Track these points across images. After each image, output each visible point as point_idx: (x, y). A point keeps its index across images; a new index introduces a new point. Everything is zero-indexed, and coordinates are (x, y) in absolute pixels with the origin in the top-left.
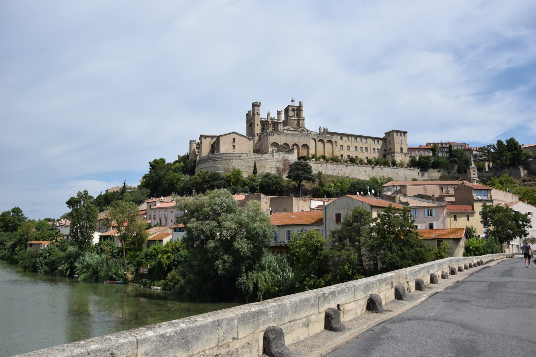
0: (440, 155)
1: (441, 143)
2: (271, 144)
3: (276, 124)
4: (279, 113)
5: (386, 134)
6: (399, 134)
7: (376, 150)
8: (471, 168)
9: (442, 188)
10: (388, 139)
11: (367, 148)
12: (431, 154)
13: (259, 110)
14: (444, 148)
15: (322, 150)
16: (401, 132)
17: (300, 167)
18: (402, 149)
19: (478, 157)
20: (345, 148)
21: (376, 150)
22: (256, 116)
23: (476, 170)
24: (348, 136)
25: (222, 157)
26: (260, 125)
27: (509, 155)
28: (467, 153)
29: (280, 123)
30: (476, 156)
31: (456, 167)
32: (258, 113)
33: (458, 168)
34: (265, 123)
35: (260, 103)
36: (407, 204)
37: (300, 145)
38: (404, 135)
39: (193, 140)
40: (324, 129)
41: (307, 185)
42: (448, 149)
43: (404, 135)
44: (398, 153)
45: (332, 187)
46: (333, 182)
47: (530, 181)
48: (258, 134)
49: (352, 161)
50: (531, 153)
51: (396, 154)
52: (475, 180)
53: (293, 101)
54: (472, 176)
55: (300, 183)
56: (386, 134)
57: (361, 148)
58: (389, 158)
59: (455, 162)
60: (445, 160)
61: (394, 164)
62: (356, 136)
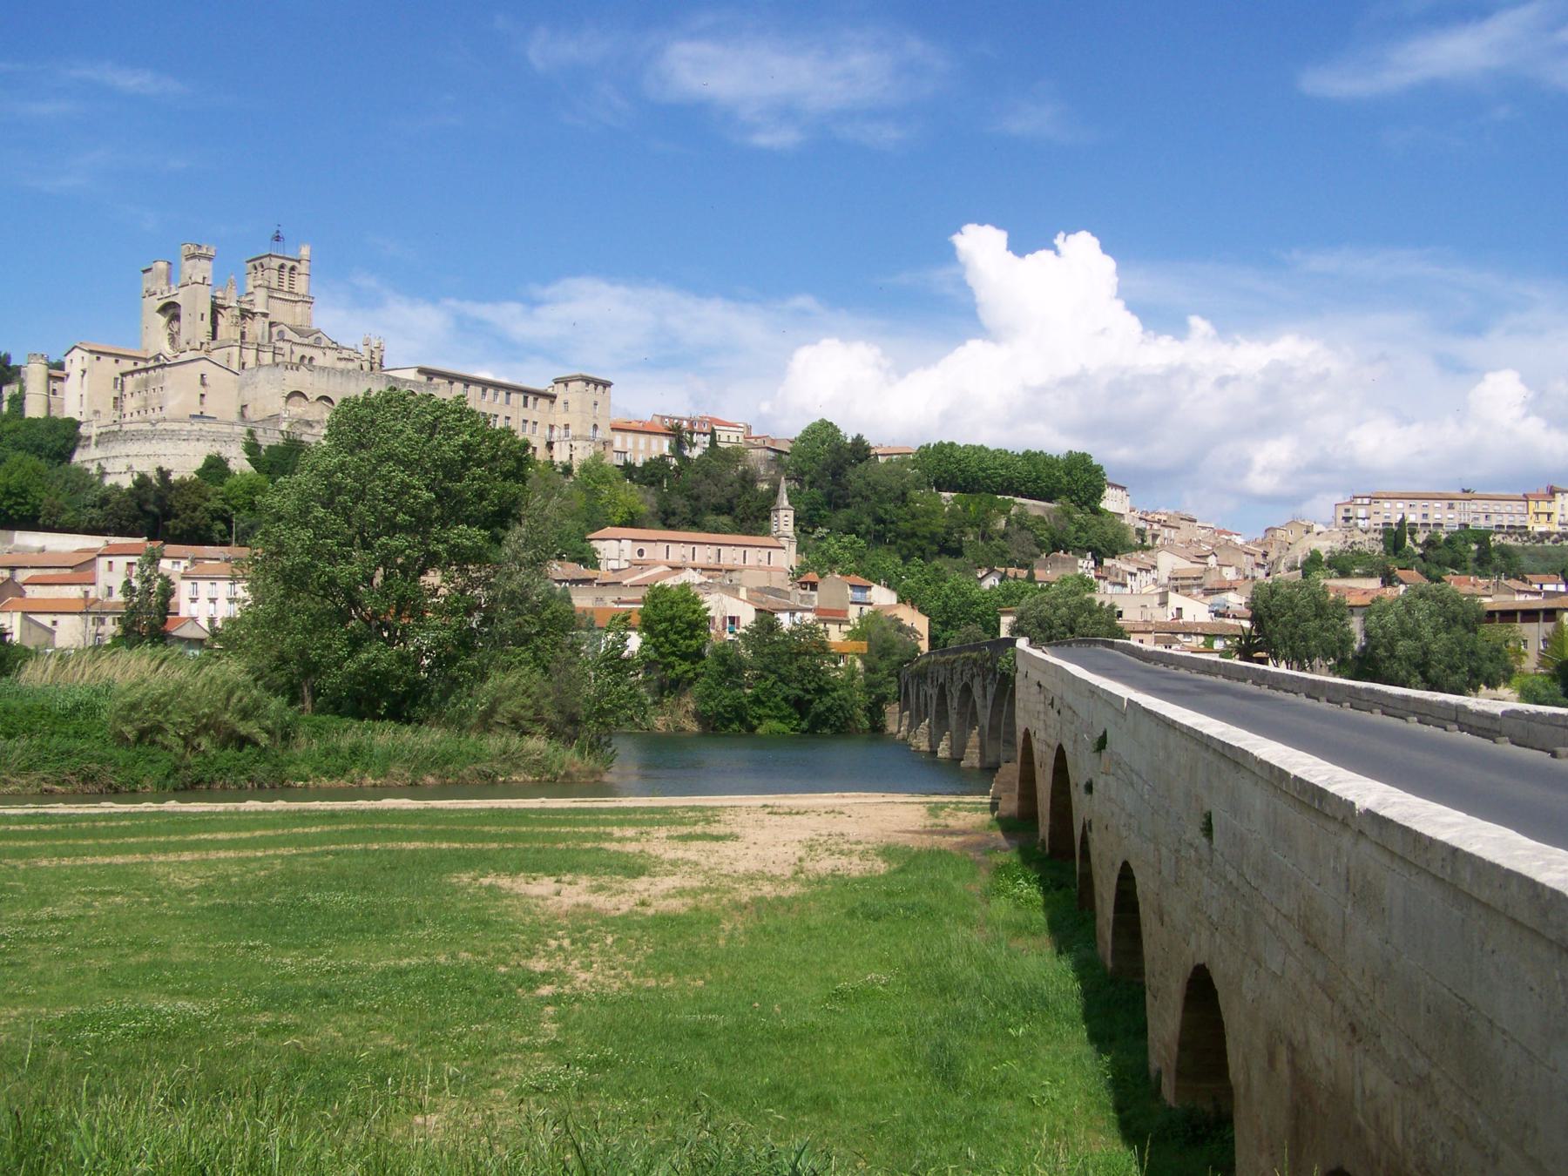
16: (598, 383)
53: (278, 238)
54: (782, 527)
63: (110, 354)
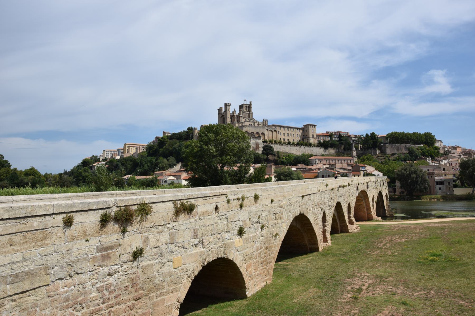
0: (334, 139)
3: (239, 117)
4: (240, 111)
6: (312, 126)
7: (299, 136)
9: (339, 161)
10: (305, 129)
11: (294, 134)
12: (329, 139)
13: (230, 108)
14: (336, 135)
15: (271, 136)
17: (269, 148)
18: (313, 135)
19: (355, 142)
20: (282, 134)
21: (299, 136)
22: (228, 112)
24: (284, 127)
26: (230, 118)
27: (371, 142)
28: (349, 138)
29: (241, 116)
30: (353, 140)
31: (343, 147)
32: (229, 110)
33: (344, 147)
35: (230, 104)
36: (339, 171)
37: (260, 133)
38: (315, 127)
40: (266, 120)
41: (270, 157)
42: (338, 136)
43: (315, 127)
44: (311, 138)
45: (284, 159)
46: (284, 156)
47: (381, 157)
49: (289, 143)
50: (383, 141)
51: (310, 139)
53: (245, 101)
54: (353, 154)
55: (267, 156)
56: (304, 126)
57: (291, 134)
58: (306, 141)
59: (342, 144)
60: (337, 143)
61: (310, 145)
62: (288, 127)
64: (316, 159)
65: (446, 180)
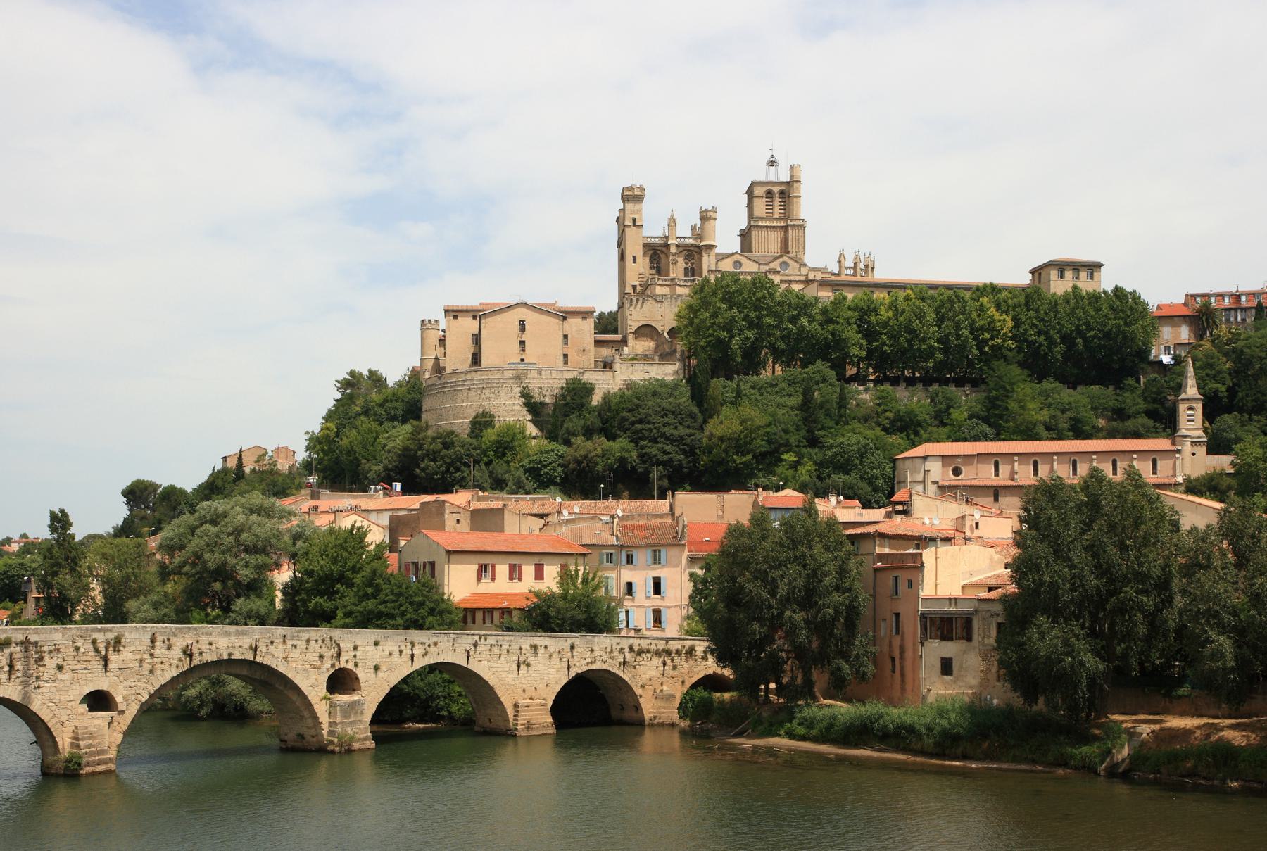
1: (1231, 295)
2: (634, 329)
5: (1033, 272)
8: (1183, 400)
13: (639, 211)
23: (1200, 406)
25: (473, 380)
32: (634, 220)
34: (662, 251)
39: (430, 321)
48: (634, 287)
52: (1186, 436)
53: (772, 163)
56: (1033, 272)
63: (467, 311)
64: (925, 458)
65: (985, 607)
